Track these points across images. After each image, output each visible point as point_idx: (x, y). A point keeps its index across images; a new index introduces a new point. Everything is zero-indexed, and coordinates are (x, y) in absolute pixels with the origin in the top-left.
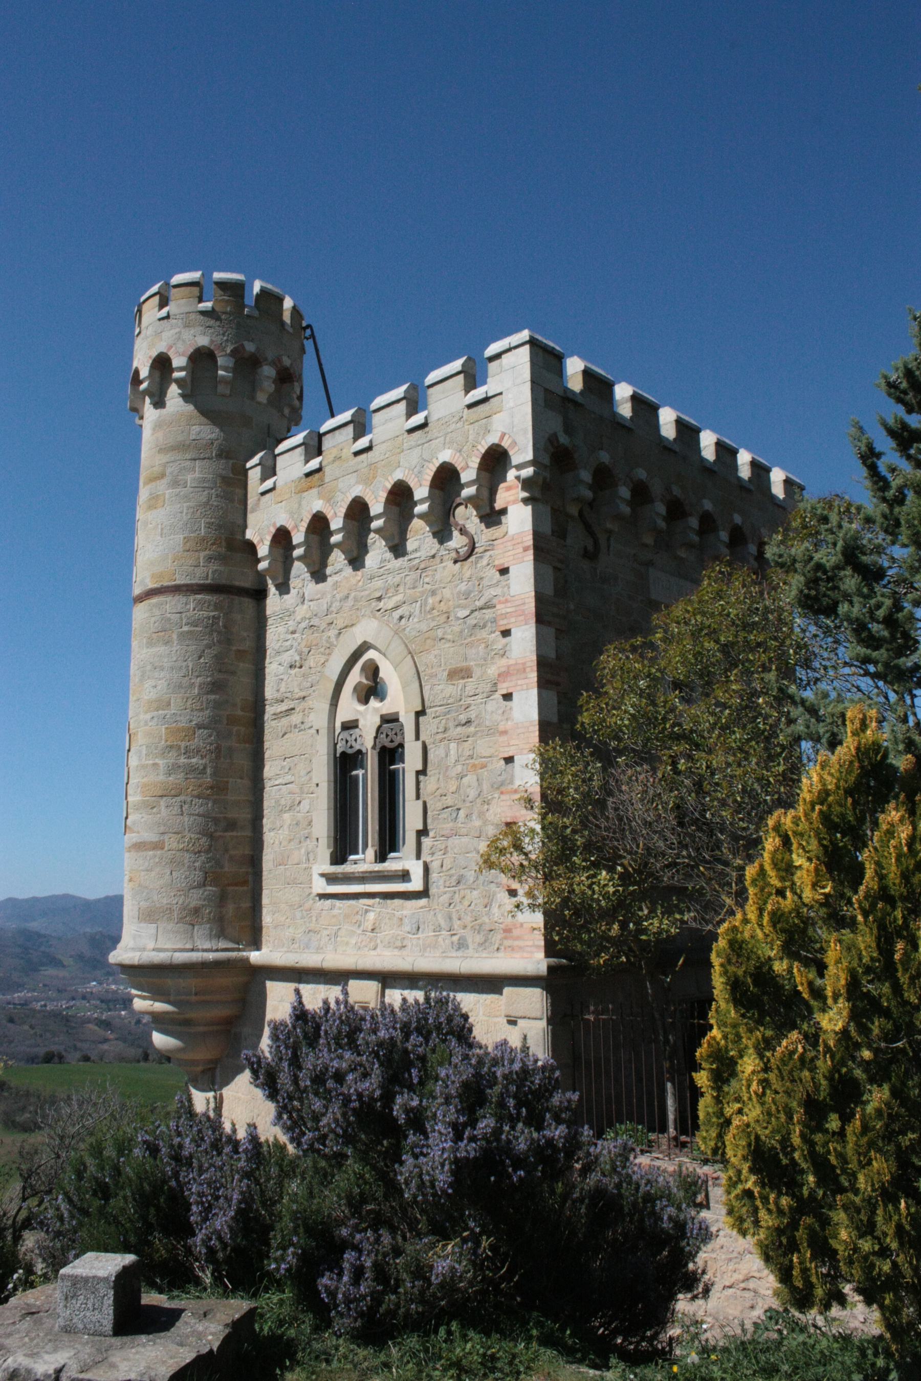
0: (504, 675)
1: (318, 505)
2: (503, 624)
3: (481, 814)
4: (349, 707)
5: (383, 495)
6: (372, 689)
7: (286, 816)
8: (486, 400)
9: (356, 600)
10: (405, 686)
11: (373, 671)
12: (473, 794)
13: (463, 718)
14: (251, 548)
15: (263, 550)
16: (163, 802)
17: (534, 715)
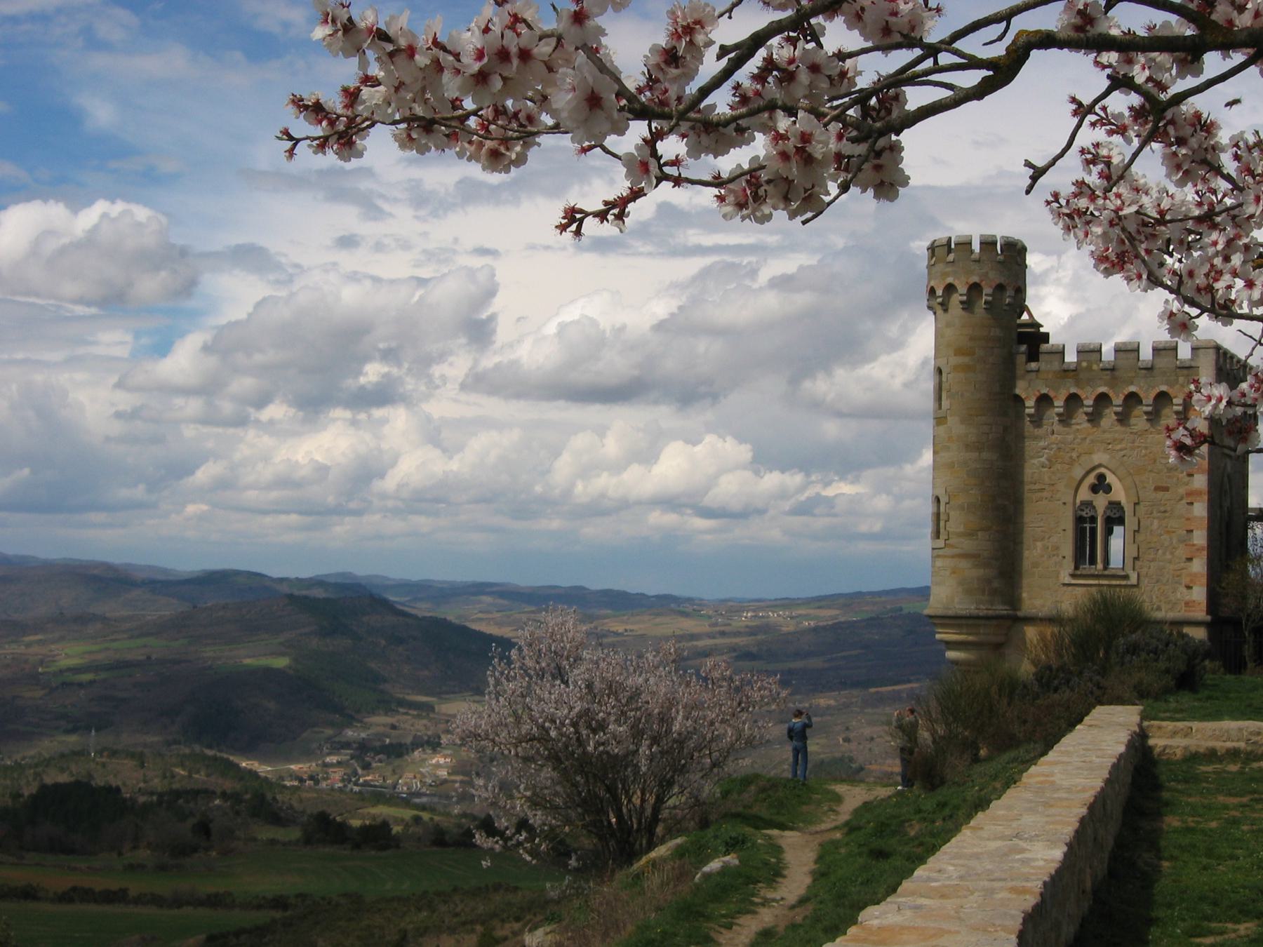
0: (1189, 494)
1: (1073, 390)
2: (1190, 471)
3: (1172, 553)
4: (1084, 494)
5: (1122, 397)
6: (1101, 485)
7: (1039, 544)
8: (1190, 367)
9: (1092, 441)
10: (1126, 490)
11: (1101, 477)
12: (1166, 544)
13: (1162, 509)
14: (1019, 400)
15: (1030, 403)
16: (980, 534)
17: (1205, 514)
